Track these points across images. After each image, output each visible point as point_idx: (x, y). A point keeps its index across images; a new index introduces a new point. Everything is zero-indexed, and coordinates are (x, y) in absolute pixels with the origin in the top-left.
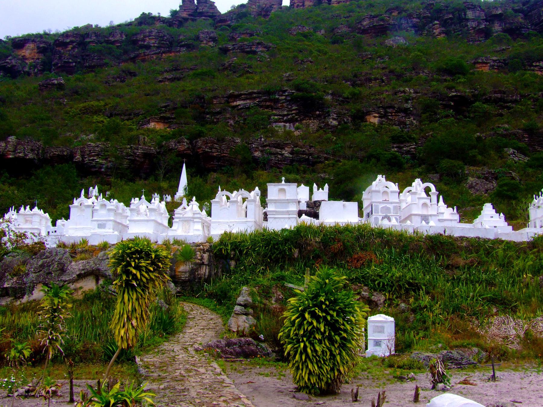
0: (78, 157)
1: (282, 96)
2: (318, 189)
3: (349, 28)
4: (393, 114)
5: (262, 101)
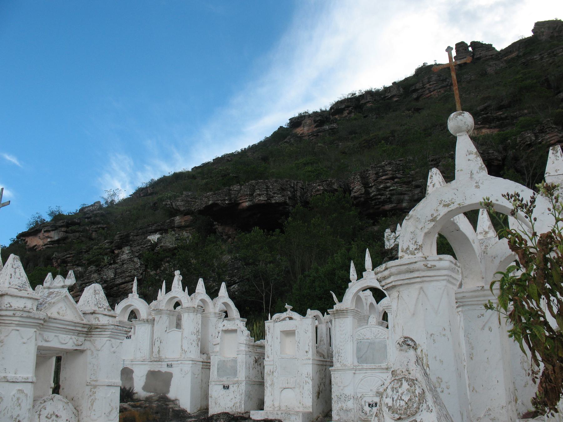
0: (357, 188)
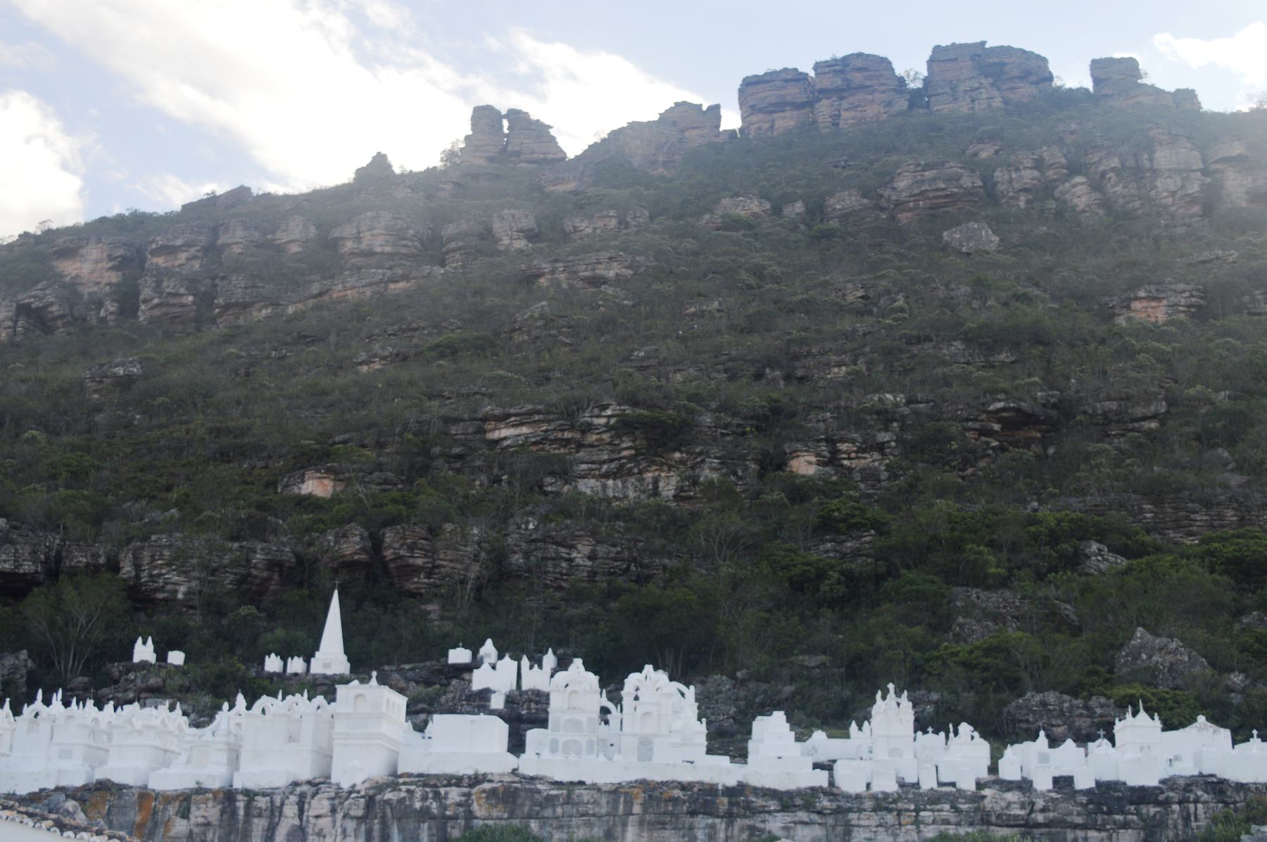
0: (127, 569)
1: (598, 416)
2: (531, 667)
3: (864, 196)
4: (853, 455)
5: (554, 430)
